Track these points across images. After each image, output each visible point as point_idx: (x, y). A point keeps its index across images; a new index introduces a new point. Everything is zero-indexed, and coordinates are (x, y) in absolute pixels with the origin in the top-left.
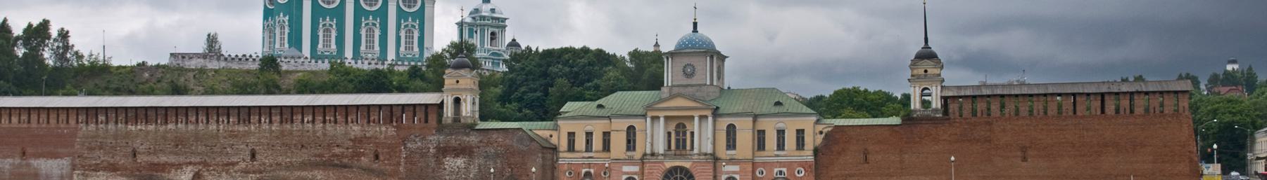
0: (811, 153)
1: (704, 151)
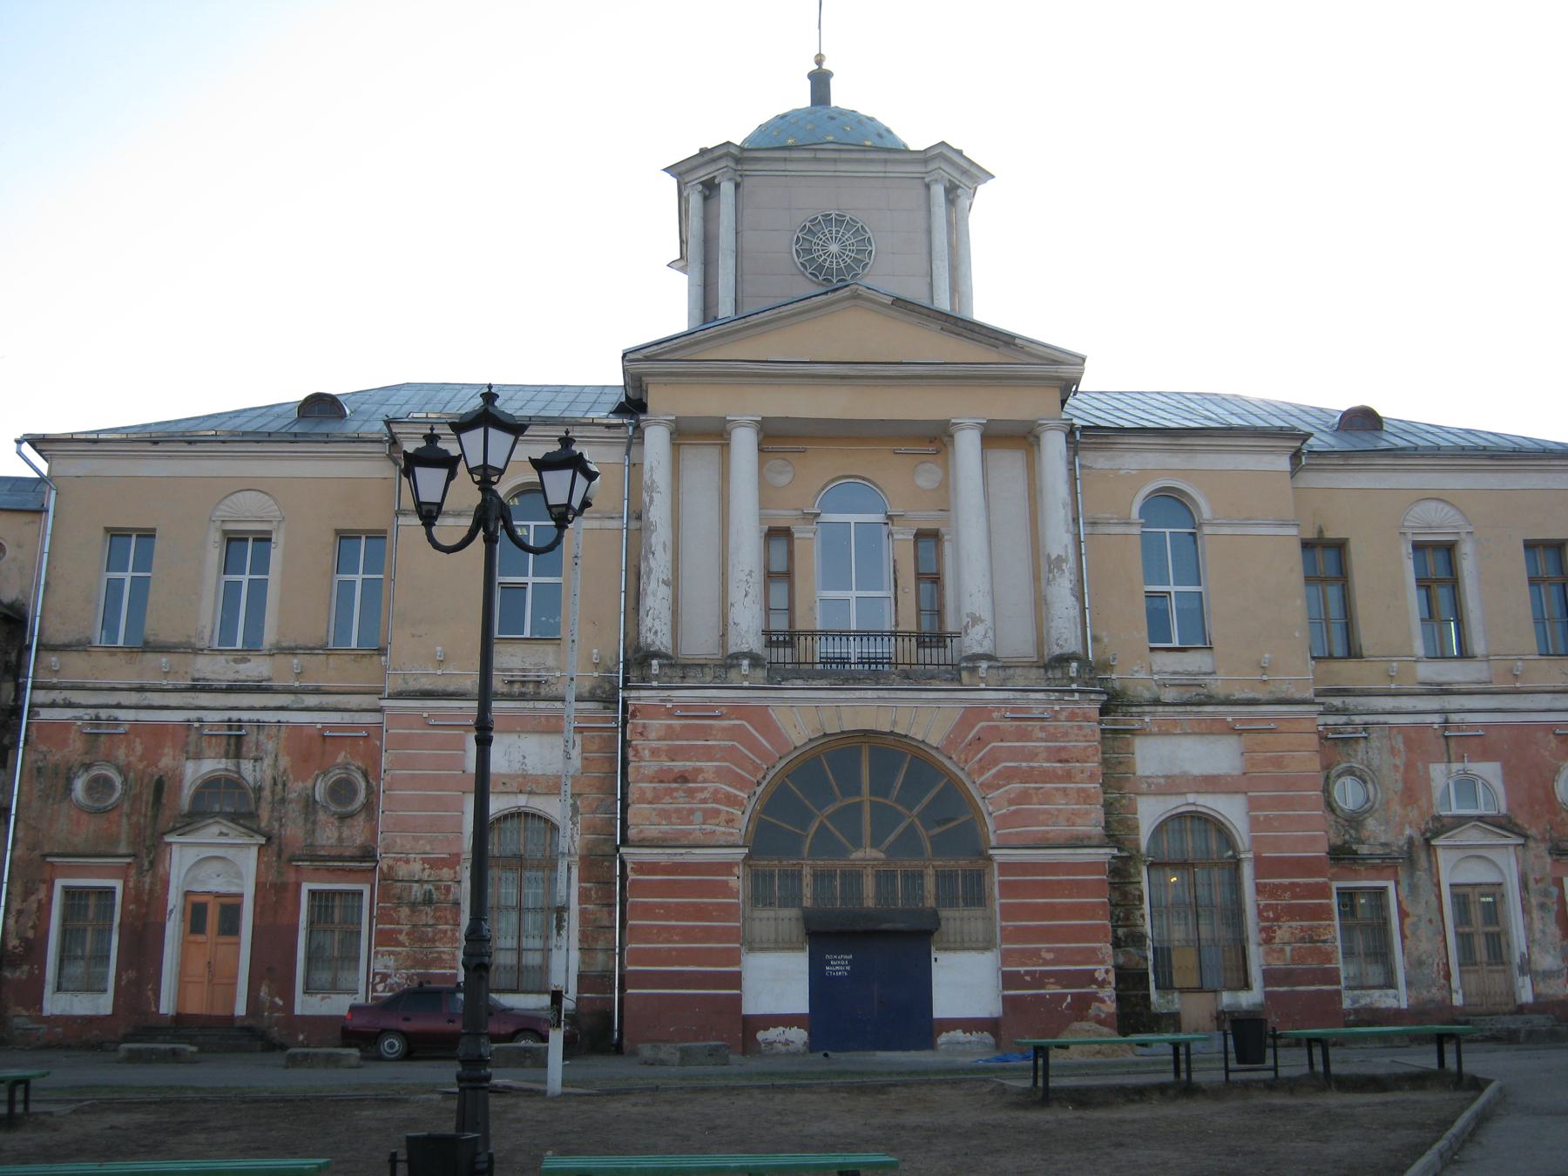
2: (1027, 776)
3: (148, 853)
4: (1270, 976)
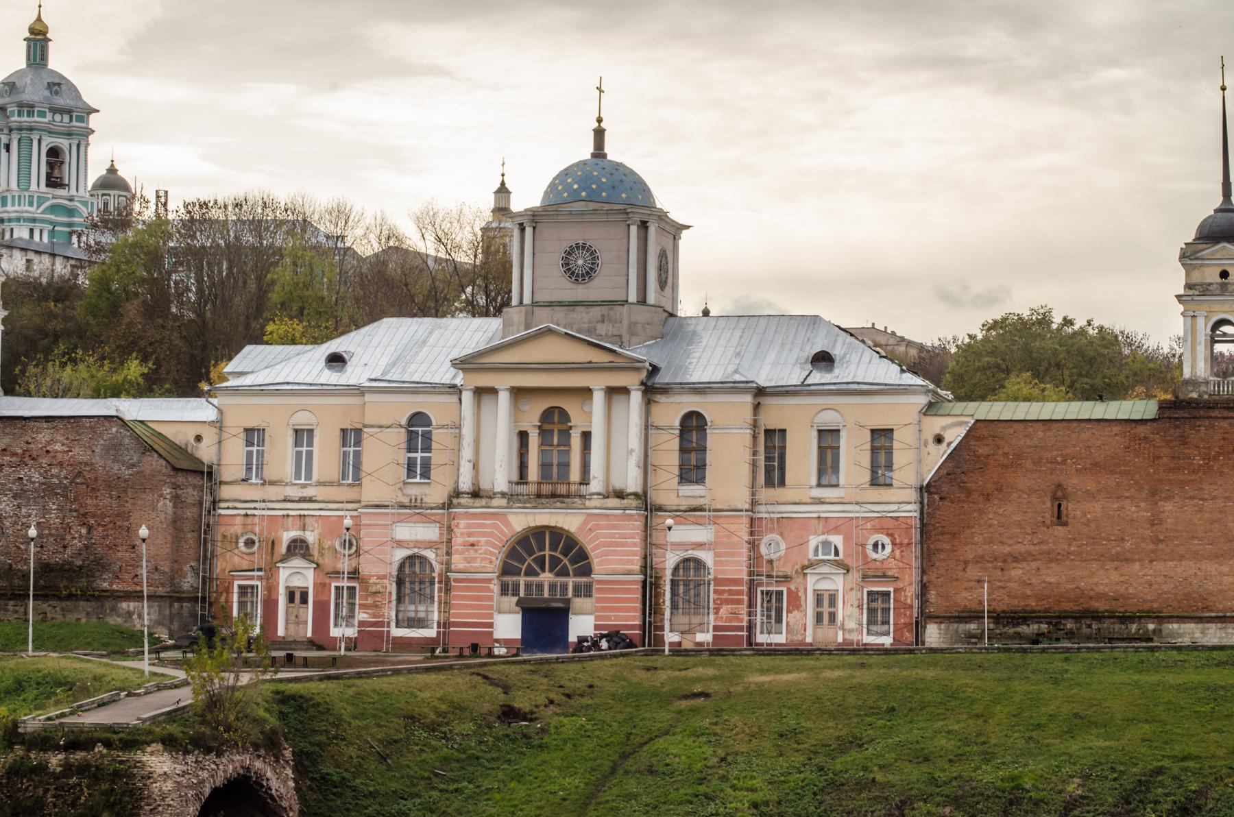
0: (913, 495)
1: (617, 484)
2: (610, 544)
3: (270, 571)
4: (716, 628)
